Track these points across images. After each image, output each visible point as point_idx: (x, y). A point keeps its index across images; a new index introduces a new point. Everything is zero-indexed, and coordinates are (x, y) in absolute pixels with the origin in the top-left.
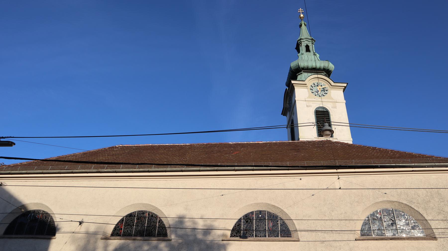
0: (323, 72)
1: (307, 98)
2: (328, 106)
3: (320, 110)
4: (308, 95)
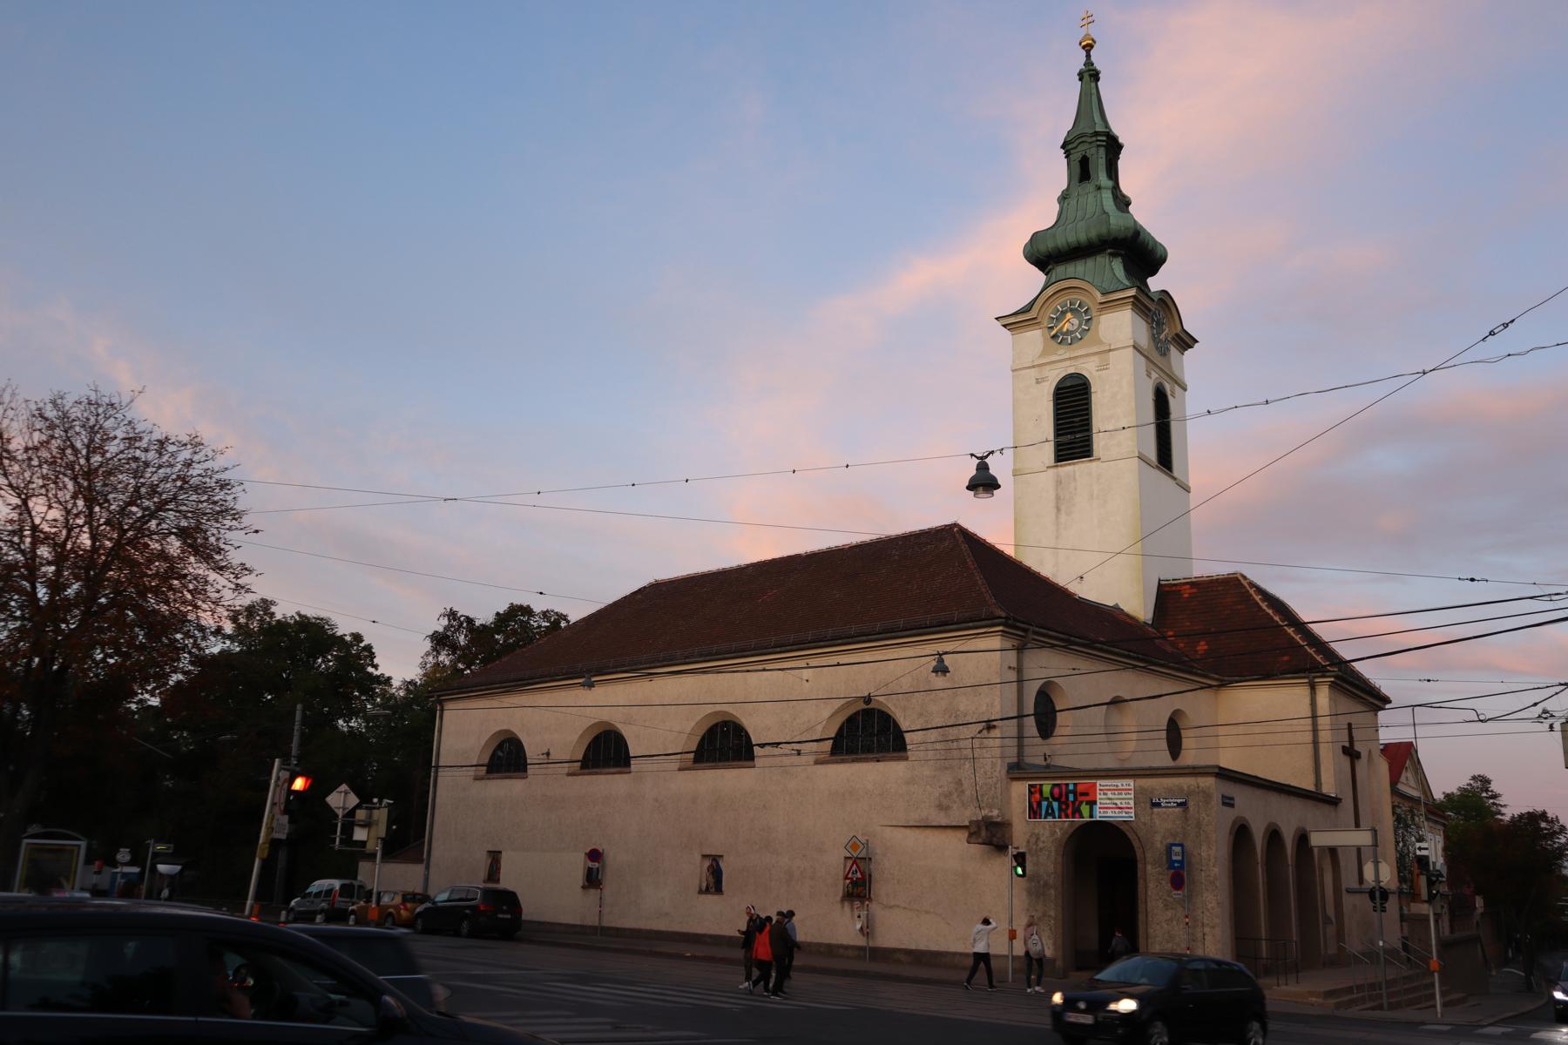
0: (1105, 250)
2: (1088, 368)
3: (1069, 385)
4: (1041, 348)
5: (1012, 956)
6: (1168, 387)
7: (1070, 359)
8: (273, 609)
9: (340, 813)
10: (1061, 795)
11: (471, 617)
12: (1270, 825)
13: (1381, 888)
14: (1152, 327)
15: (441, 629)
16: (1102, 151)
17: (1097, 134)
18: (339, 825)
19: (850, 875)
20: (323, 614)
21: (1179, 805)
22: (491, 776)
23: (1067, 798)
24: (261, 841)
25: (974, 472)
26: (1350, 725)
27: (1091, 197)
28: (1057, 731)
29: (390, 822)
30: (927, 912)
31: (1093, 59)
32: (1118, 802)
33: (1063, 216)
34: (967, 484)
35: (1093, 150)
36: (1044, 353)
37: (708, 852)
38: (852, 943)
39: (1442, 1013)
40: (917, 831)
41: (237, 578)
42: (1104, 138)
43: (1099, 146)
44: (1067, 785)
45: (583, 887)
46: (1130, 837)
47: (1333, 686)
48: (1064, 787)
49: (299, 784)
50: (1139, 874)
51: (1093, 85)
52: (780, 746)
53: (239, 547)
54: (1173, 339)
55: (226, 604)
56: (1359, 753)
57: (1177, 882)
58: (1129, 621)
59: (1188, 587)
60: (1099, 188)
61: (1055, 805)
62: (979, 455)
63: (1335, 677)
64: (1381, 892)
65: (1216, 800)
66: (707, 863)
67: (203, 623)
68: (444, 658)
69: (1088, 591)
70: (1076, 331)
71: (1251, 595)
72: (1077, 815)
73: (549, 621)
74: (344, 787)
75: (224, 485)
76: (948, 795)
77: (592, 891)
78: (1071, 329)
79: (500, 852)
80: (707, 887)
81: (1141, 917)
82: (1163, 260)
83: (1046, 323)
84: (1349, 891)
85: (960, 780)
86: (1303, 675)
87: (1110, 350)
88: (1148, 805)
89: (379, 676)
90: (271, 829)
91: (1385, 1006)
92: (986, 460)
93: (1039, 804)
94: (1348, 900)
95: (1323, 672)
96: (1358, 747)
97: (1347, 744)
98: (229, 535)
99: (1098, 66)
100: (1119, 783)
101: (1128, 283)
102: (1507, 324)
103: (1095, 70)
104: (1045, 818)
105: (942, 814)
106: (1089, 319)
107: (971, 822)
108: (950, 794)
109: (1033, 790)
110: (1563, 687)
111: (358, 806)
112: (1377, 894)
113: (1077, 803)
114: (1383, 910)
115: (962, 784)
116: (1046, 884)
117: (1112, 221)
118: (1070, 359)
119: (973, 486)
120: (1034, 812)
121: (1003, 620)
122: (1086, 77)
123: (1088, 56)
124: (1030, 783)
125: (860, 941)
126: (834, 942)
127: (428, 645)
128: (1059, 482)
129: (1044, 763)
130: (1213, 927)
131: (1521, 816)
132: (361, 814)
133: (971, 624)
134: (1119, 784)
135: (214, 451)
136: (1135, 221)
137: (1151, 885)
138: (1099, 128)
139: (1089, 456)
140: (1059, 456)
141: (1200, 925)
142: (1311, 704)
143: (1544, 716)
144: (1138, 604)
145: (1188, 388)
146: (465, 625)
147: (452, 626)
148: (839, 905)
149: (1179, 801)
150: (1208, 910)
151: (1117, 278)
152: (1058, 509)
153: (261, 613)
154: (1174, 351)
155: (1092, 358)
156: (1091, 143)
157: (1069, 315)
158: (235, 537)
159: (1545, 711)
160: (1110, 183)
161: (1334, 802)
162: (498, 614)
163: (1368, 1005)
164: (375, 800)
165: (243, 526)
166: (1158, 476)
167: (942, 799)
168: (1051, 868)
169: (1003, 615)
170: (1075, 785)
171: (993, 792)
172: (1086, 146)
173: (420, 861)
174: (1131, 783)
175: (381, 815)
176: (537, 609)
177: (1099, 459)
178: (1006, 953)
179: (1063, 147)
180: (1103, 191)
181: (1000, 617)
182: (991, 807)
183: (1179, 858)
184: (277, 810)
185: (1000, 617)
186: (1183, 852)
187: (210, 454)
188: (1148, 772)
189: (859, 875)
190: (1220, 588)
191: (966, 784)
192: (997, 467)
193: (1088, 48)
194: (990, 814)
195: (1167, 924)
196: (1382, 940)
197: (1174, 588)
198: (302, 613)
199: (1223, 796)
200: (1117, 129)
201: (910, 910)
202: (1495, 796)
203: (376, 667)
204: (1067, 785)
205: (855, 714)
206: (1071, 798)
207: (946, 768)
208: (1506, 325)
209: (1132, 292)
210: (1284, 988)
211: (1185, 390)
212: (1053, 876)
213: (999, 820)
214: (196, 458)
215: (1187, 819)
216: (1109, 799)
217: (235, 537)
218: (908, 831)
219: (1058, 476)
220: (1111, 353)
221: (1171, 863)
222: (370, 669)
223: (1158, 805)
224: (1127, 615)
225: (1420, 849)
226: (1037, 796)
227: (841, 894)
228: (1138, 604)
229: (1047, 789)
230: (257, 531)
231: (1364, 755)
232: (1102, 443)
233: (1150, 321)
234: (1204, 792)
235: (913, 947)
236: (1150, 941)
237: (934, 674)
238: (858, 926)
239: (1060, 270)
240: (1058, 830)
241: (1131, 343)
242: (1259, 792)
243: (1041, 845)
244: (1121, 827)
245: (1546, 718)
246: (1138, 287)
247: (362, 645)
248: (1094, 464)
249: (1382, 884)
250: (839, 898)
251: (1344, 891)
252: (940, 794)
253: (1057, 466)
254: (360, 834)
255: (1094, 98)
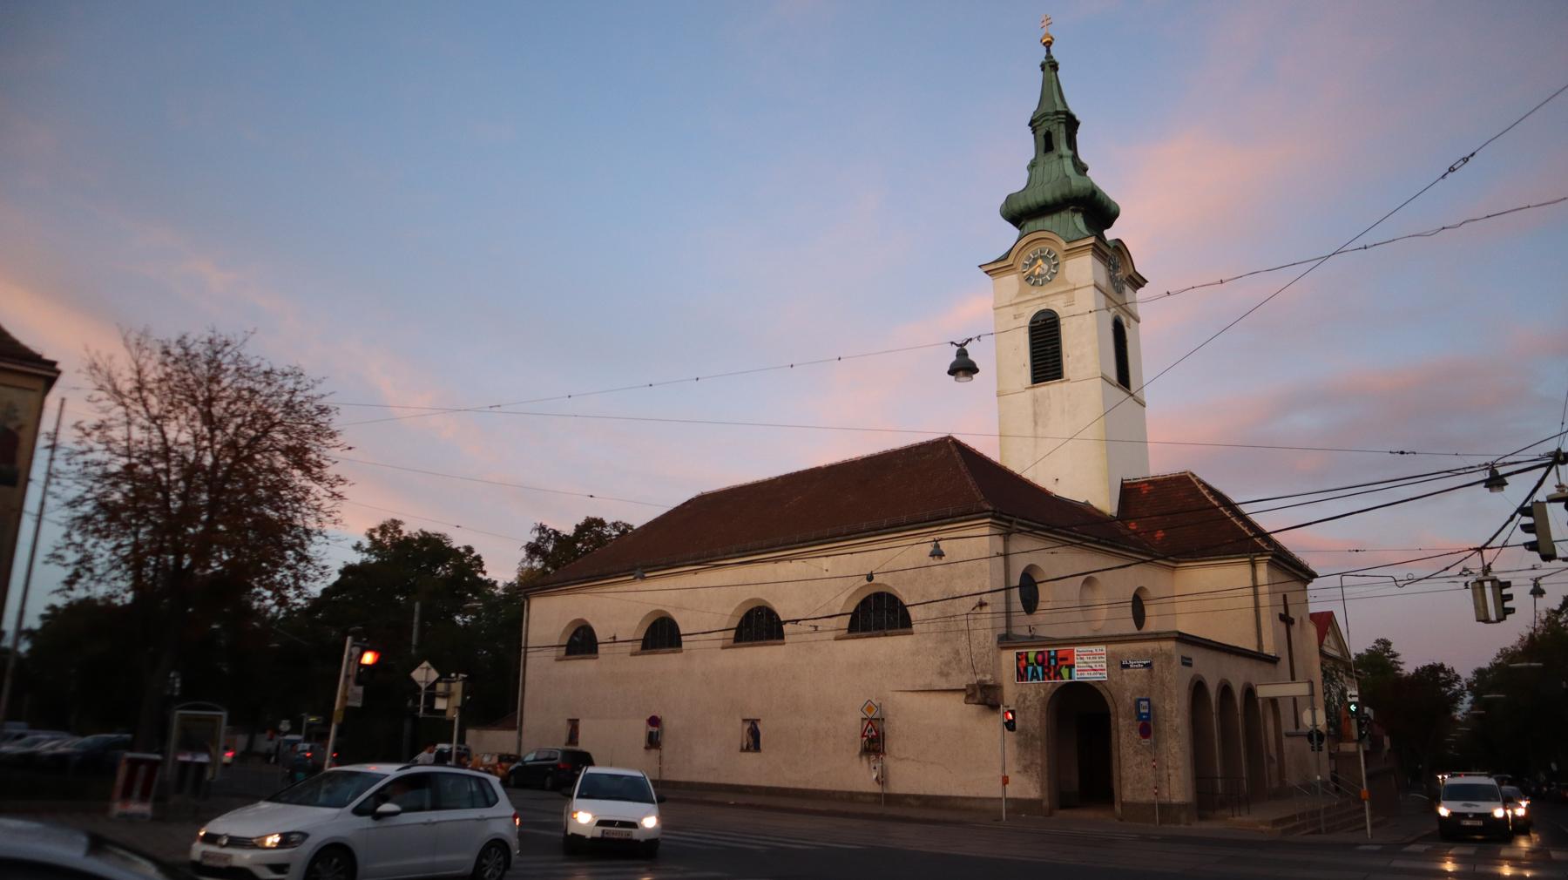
0: (1068, 207)
1: (1017, 296)
2: (1058, 305)
5: (1006, 799)
6: (1124, 320)
7: (1042, 297)
8: (401, 527)
9: (423, 686)
10: (1044, 660)
11: (557, 530)
12: (1221, 683)
13: (1318, 731)
14: (1109, 270)
15: (534, 541)
16: (1062, 127)
17: (1057, 113)
18: (423, 697)
19: (866, 733)
20: (440, 531)
21: (1145, 666)
22: (569, 657)
23: (1049, 663)
24: (337, 707)
25: (954, 358)
26: (1285, 596)
27: (1055, 165)
28: (1040, 606)
29: (464, 693)
30: (932, 763)
31: (1052, 53)
32: (1093, 665)
33: (1032, 183)
34: (948, 369)
35: (1056, 126)
36: (1020, 293)
37: (748, 717)
38: (869, 790)
39: (1372, 835)
40: (922, 694)
41: (332, 487)
42: (1063, 116)
43: (1059, 123)
44: (1049, 652)
45: (646, 748)
46: (1104, 694)
47: (1270, 563)
48: (1046, 654)
49: (368, 658)
50: (1112, 727)
51: (1053, 74)
52: (799, 623)
53: (336, 462)
54: (1126, 279)
55: (326, 510)
56: (1293, 619)
57: (1145, 731)
58: (1097, 514)
59: (1146, 485)
60: (1061, 157)
61: (1039, 669)
62: (957, 343)
63: (1272, 556)
64: (1317, 735)
65: (1177, 660)
66: (747, 726)
67: (308, 527)
68: (537, 564)
69: (1063, 491)
70: (1046, 274)
71: (1199, 490)
72: (1058, 677)
73: (619, 530)
74: (426, 664)
75: (323, 410)
76: (948, 664)
77: (653, 751)
78: (1042, 272)
79: (578, 720)
80: (748, 747)
81: (1115, 763)
82: (1116, 215)
83: (1020, 268)
84: (1288, 735)
85: (958, 651)
86: (1245, 555)
87: (1075, 289)
88: (1119, 666)
89: (486, 581)
90: (345, 698)
91: (1323, 829)
92: (966, 347)
93: (1026, 669)
94: (1287, 742)
95: (1262, 552)
96: (1291, 615)
97: (1283, 612)
98: (328, 452)
99: (1056, 58)
100: (1093, 648)
101: (1087, 233)
102: (1467, 159)
103: (1054, 62)
104: (1031, 680)
105: (944, 680)
106: (1057, 264)
107: (967, 686)
108: (950, 662)
109: (1020, 657)
110: (1472, 552)
111: (438, 680)
112: (1315, 736)
113: (1058, 667)
114: (1320, 749)
115: (959, 654)
116: (1032, 736)
117: (1073, 183)
118: (1042, 297)
119: (953, 371)
120: (1021, 676)
121: (990, 513)
122: (1047, 68)
123: (1048, 51)
124: (1018, 651)
125: (877, 789)
126: (854, 789)
127: (523, 554)
128: (1035, 400)
129: (1029, 634)
130: (1176, 769)
131: (1424, 668)
132: (441, 687)
133: (963, 518)
134: (1094, 650)
135: (313, 381)
136: (1092, 183)
137: (1123, 735)
138: (1060, 108)
139: (1060, 378)
140: (1035, 378)
141: (1165, 767)
142: (1253, 579)
143: (1465, 573)
144: (1105, 501)
145: (1141, 320)
146: (553, 536)
147: (543, 538)
148: (858, 759)
149: (1145, 662)
150: (1171, 754)
151: (1079, 230)
152: (1036, 423)
153: (391, 530)
154: (1128, 290)
155: (1060, 296)
156: (1053, 120)
157: (1040, 262)
158: (334, 453)
159: (1465, 569)
160: (1070, 153)
161: (1273, 660)
162: (577, 526)
163: (1310, 830)
164: (453, 675)
165: (339, 443)
166: (1120, 394)
167: (943, 667)
168: (1037, 724)
169: (991, 508)
170: (1056, 651)
171: (985, 660)
172: (1049, 123)
173: (514, 728)
174: (1103, 648)
175: (457, 687)
176: (608, 520)
177: (1069, 380)
178: (1000, 796)
179: (1030, 124)
180: (1065, 159)
181: (988, 511)
182: (984, 672)
183: (1147, 711)
184: (351, 681)
185: (988, 511)
186: (1149, 704)
187: (310, 383)
188: (1117, 639)
189: (874, 733)
190: (1174, 485)
191: (963, 654)
192: (973, 354)
193: (1048, 45)
194: (984, 679)
195: (1138, 768)
196: (1319, 774)
197: (1135, 486)
198: (425, 530)
199: (1183, 657)
200: (1073, 109)
201: (919, 762)
202: (1395, 656)
203: (484, 573)
204: (1049, 652)
205: (867, 597)
206: (1053, 662)
207: (946, 641)
208: (1466, 160)
209: (1092, 240)
210: (1237, 818)
211: (1138, 322)
212: (1038, 730)
213: (992, 683)
214: (299, 387)
215: (1152, 678)
216: (1085, 663)
217: (334, 453)
218: (915, 696)
219: (1034, 395)
220: (1076, 291)
221: (1139, 715)
222: (480, 575)
223: (1127, 666)
224: (1096, 510)
225: (1351, 696)
226: (1024, 662)
227: (859, 750)
228: (1105, 501)
229: (1032, 656)
230: (350, 448)
231: (1297, 621)
232: (1070, 367)
233: (1107, 264)
234: (1166, 654)
235: (922, 793)
236: (1123, 782)
237: (931, 558)
238: (875, 776)
239: (1031, 225)
240: (1042, 691)
241: (1092, 282)
242: (1212, 654)
243: (1028, 703)
244: (1096, 686)
245: (1466, 576)
246: (1097, 236)
247: (473, 555)
248: (1065, 384)
249: (1318, 728)
250: (857, 753)
251: (1284, 736)
252: (941, 663)
253: (1034, 387)
254: (440, 704)
255: (1055, 83)
